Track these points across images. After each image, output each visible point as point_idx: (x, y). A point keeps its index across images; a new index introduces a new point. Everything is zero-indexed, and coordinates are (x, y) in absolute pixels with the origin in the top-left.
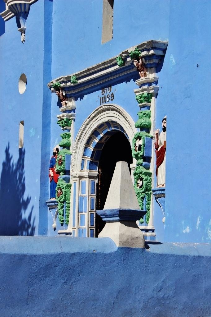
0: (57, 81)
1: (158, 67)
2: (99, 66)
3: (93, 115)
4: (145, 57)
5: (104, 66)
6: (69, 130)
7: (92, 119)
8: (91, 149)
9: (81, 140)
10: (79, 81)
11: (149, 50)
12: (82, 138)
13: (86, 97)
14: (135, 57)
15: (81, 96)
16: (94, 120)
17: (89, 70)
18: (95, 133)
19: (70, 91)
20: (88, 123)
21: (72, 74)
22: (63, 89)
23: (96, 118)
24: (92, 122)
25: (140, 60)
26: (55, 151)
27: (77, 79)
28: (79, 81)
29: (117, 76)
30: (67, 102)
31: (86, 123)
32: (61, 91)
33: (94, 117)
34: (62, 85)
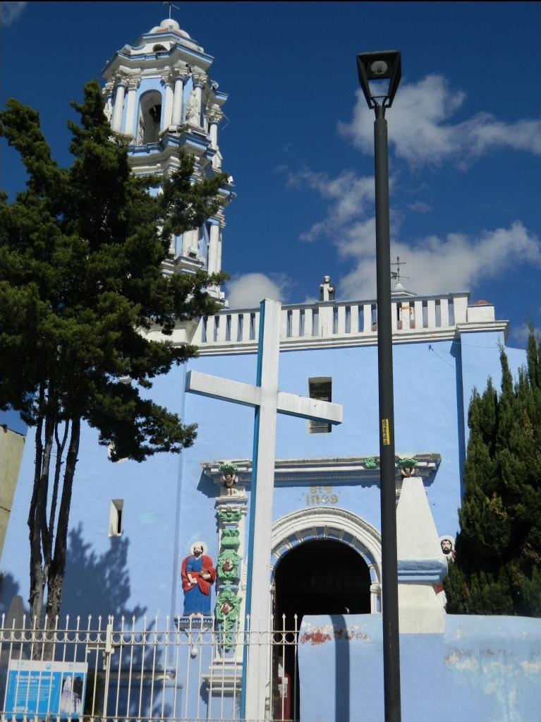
0: (233, 462)
2: (328, 460)
3: (295, 515)
4: (420, 468)
5: (336, 463)
6: (237, 526)
7: (291, 520)
8: (278, 556)
11: (428, 462)
16: (295, 520)
17: (304, 461)
18: (292, 538)
19: (244, 478)
20: (283, 523)
22: (238, 474)
23: (299, 519)
24: (289, 523)
25: (413, 470)
26: (200, 550)
29: (351, 477)
30: (236, 490)
31: (280, 522)
32: (234, 476)
33: (296, 518)
34: (240, 469)
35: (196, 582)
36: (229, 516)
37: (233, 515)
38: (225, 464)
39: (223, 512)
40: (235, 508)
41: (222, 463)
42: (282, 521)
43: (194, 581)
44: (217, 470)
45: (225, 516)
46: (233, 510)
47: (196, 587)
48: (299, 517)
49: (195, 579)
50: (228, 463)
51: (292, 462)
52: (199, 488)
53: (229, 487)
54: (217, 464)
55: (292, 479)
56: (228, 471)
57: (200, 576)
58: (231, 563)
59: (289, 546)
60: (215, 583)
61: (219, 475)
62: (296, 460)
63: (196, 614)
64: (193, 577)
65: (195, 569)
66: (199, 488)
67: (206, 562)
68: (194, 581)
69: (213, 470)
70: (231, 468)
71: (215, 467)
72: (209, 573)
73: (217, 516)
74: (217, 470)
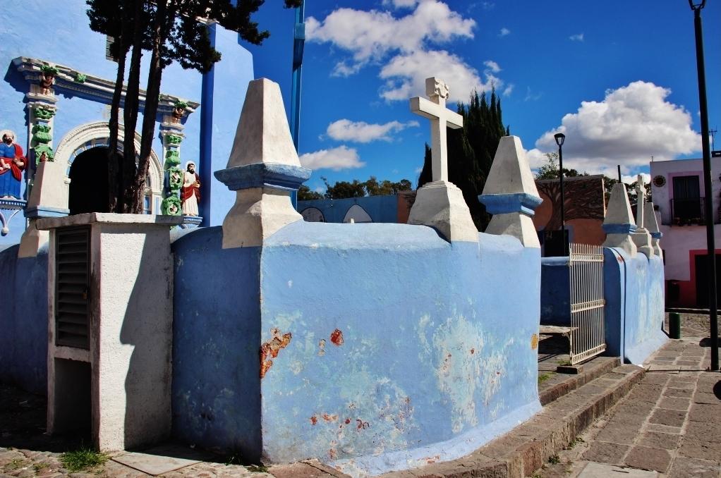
0: (57, 66)
1: (183, 121)
3: (96, 125)
7: (92, 128)
9: (69, 142)
10: (85, 83)
12: (71, 141)
13: (75, 99)
14: (183, 107)
15: (69, 95)
18: (88, 143)
21: (82, 74)
22: (58, 78)
23: (98, 129)
27: (87, 81)
28: (85, 83)
33: (96, 127)
34: (60, 74)
35: (9, 168)
36: (45, 114)
37: (48, 113)
38: (50, 66)
39: (40, 109)
40: (52, 108)
41: (45, 63)
42: (86, 127)
43: (8, 166)
44: (39, 69)
45: (41, 112)
46: (49, 109)
47: (9, 174)
48: (98, 127)
49: (8, 164)
50: (52, 65)
51: (103, 81)
52: (7, 79)
53: (46, 87)
54: (41, 63)
55: (96, 94)
56: (50, 73)
57: (13, 163)
58: (47, 155)
59: (84, 149)
60: (24, 171)
61: (39, 73)
62: (107, 80)
63: (9, 196)
64: (6, 163)
65: (8, 155)
66: (7, 79)
67: (17, 149)
68: (8, 166)
69: (35, 68)
70: (55, 71)
71: (38, 65)
72: (22, 161)
73: (26, 110)
74: (39, 69)
